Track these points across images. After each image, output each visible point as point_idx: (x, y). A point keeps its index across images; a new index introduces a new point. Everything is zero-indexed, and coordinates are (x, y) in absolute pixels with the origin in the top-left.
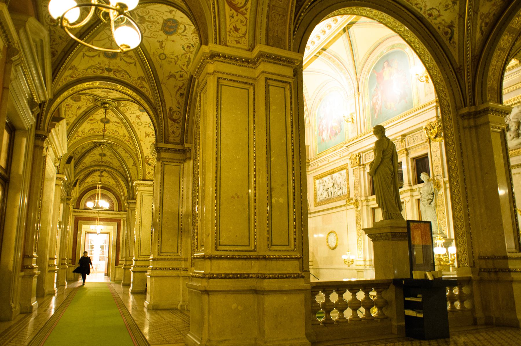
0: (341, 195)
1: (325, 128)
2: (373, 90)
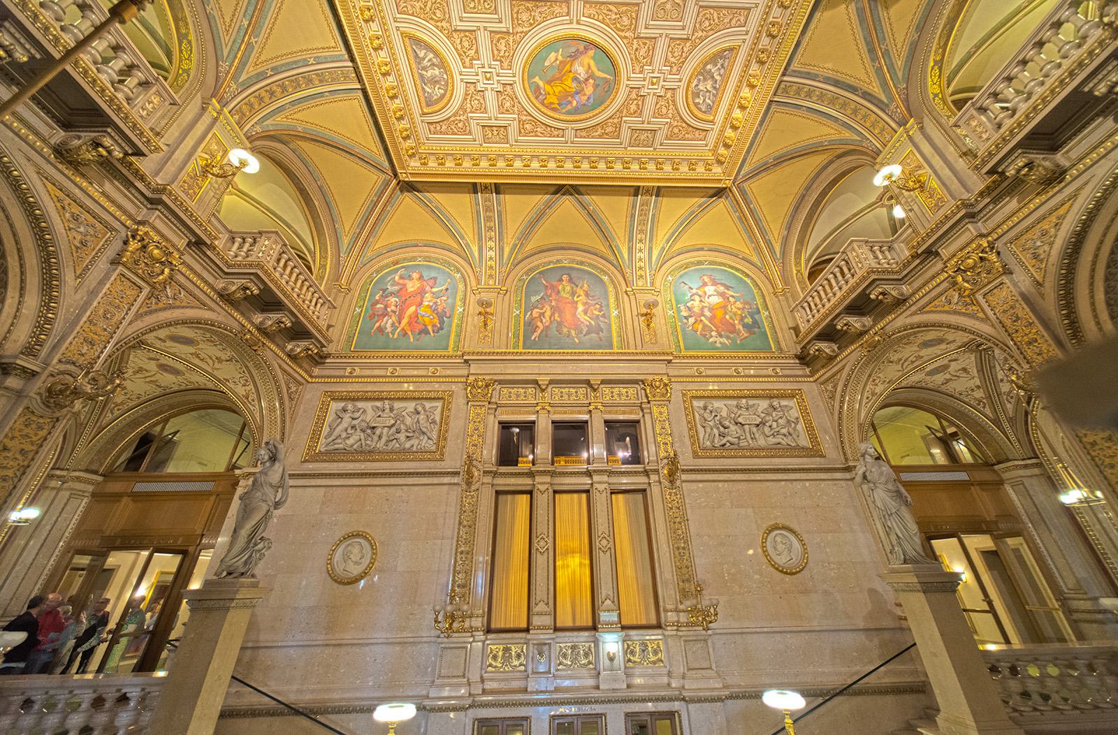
0: (414, 449)
1: (394, 312)
2: (534, 299)
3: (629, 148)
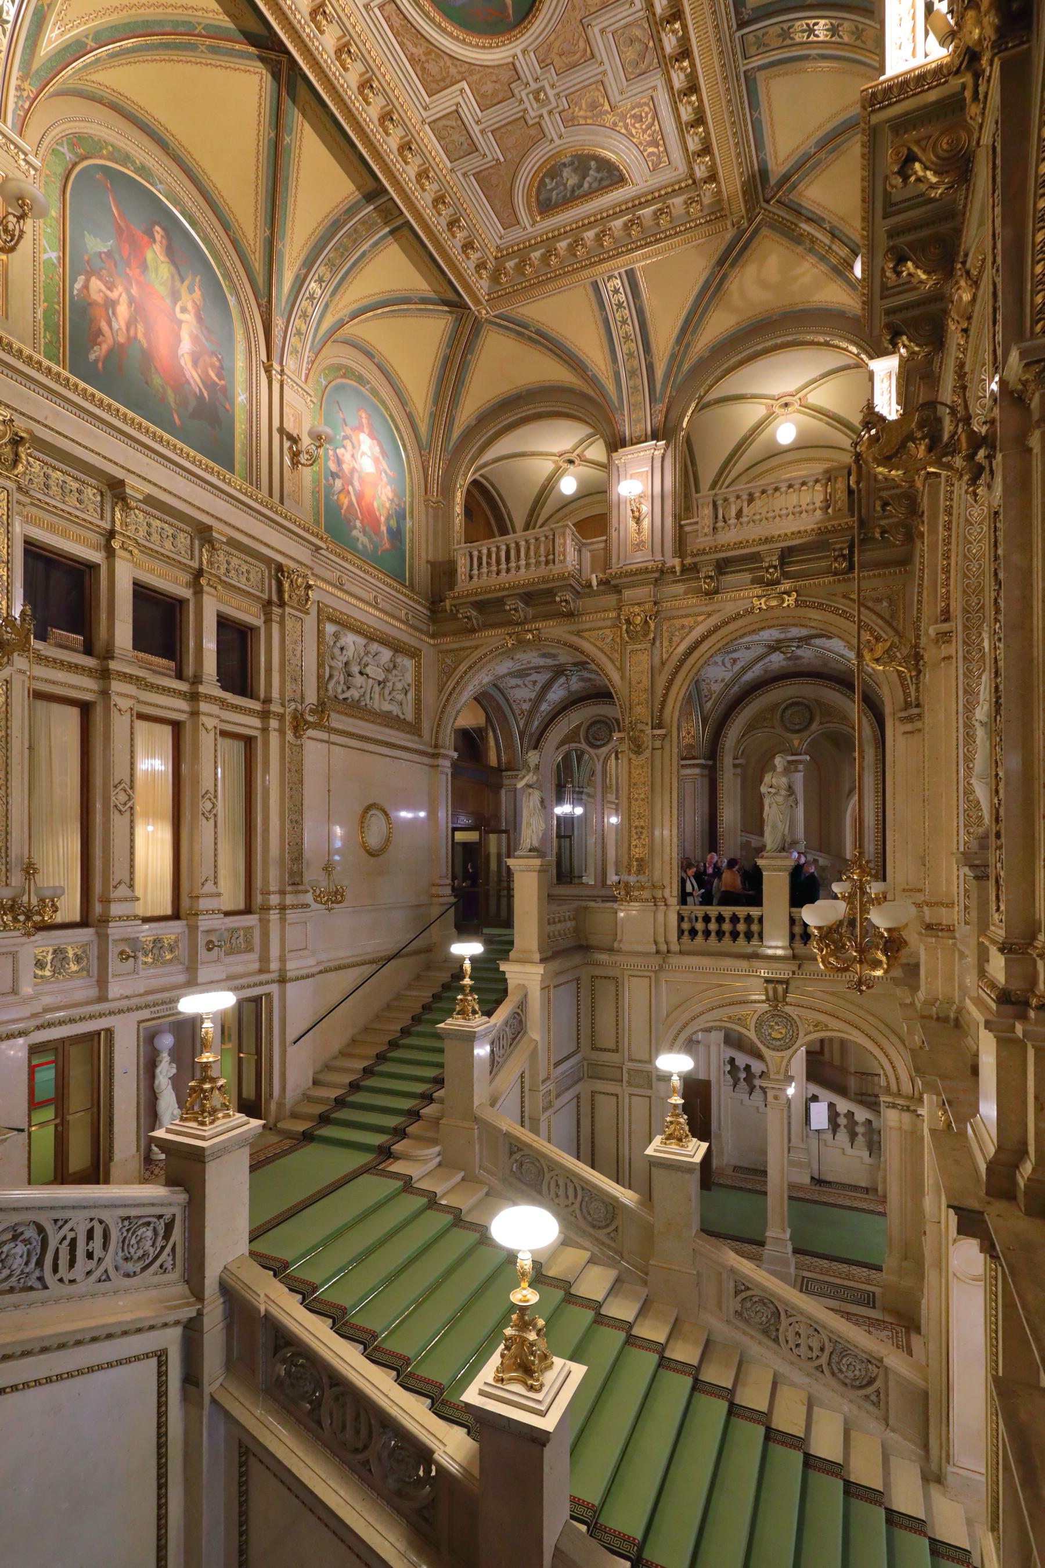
3: (427, 127)
